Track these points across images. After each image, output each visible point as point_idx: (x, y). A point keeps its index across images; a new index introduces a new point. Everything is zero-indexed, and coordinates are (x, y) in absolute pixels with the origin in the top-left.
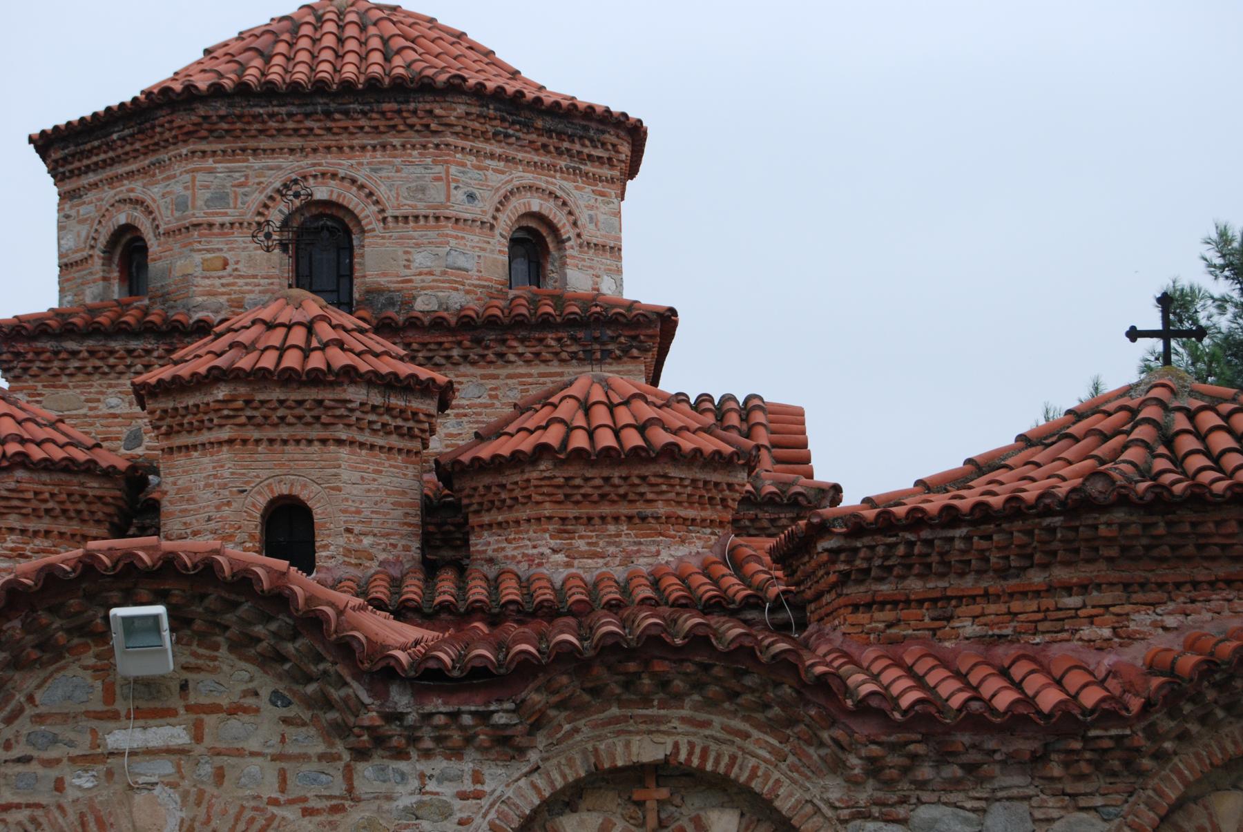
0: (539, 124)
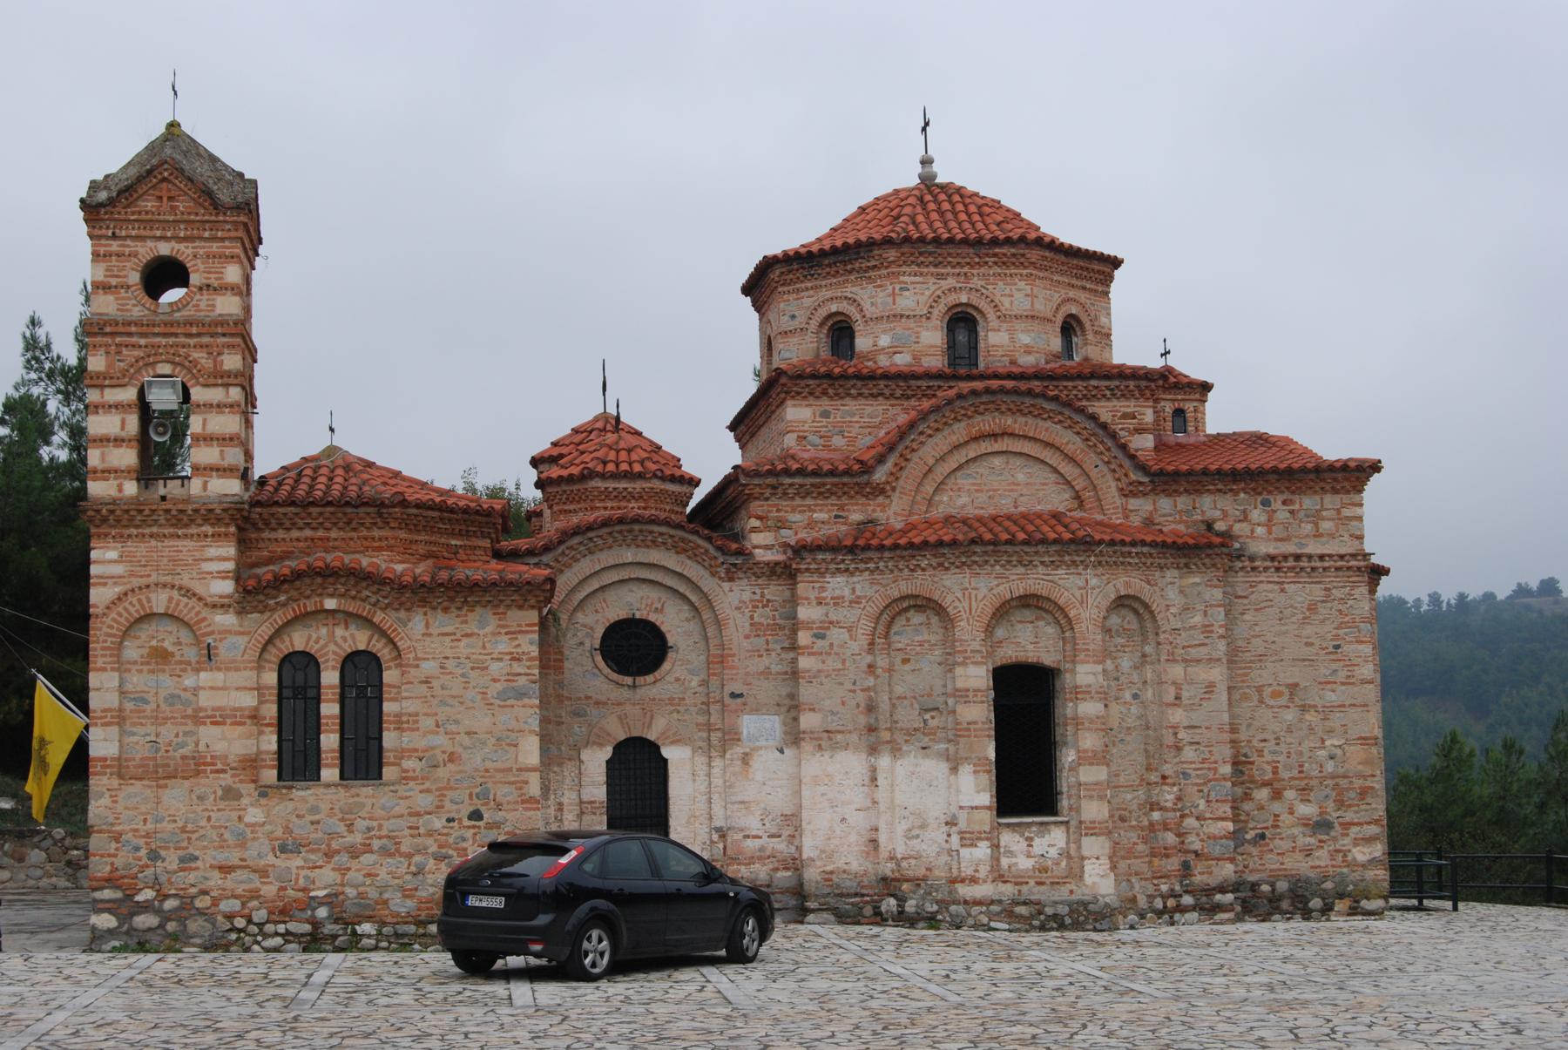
0: (826, 262)
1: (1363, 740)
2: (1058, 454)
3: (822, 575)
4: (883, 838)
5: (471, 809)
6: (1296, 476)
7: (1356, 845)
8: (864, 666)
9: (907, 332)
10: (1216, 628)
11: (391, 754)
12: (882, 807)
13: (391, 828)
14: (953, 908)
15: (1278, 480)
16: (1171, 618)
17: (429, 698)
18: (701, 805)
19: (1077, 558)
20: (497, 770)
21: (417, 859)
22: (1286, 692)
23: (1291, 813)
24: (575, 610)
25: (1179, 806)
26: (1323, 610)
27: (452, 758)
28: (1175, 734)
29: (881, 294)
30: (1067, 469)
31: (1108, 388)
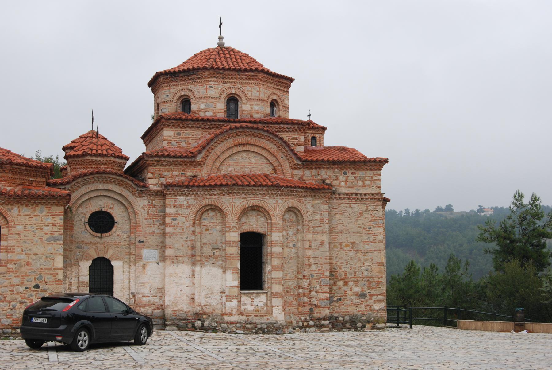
1: (379, 264)
2: (268, 152)
3: (176, 196)
4: (196, 298)
5: (35, 284)
6: (357, 163)
7: (375, 303)
8: (191, 232)
9: (211, 104)
10: (325, 220)
11: (4, 262)
12: (196, 286)
13: (2, 291)
14: (223, 325)
15: (350, 165)
16: (308, 216)
17: (19, 240)
18: (126, 284)
19: (273, 192)
20: (46, 269)
21: (13, 303)
22: (351, 245)
24: (79, 207)
26: (365, 214)
27: (28, 264)
28: (309, 260)
29: (202, 88)
30: (271, 158)
31: (287, 128)
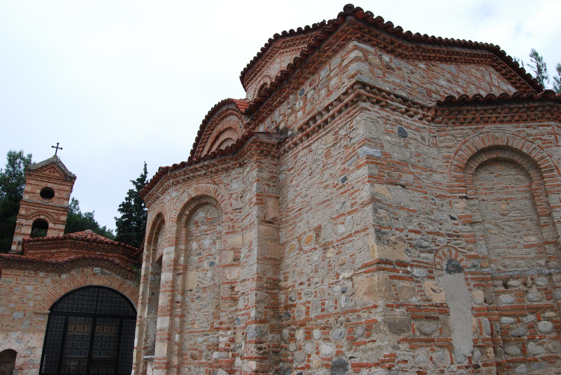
16: (233, 202)
23: (318, 353)
25: (232, 347)
26: (334, 153)
28: (233, 288)
